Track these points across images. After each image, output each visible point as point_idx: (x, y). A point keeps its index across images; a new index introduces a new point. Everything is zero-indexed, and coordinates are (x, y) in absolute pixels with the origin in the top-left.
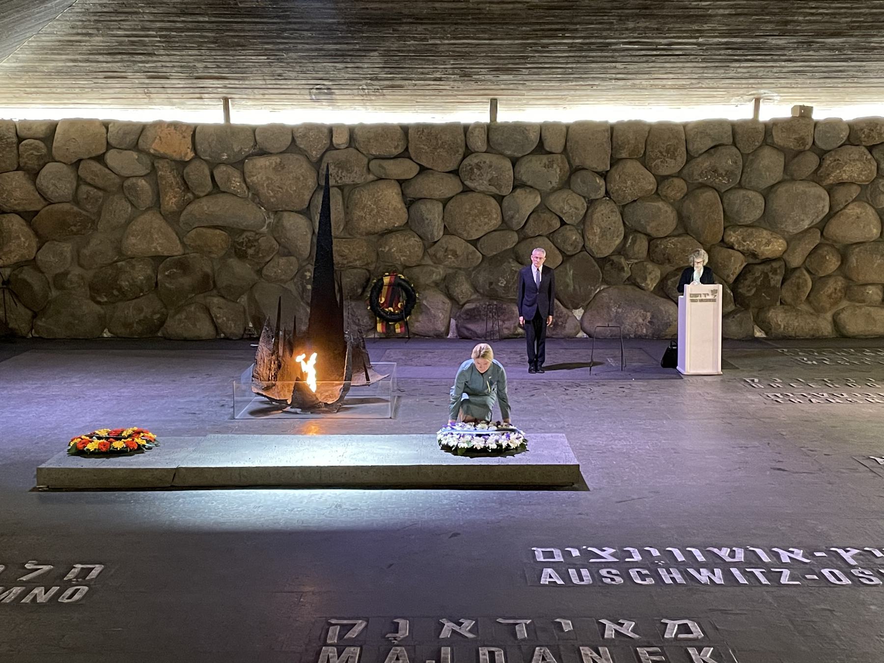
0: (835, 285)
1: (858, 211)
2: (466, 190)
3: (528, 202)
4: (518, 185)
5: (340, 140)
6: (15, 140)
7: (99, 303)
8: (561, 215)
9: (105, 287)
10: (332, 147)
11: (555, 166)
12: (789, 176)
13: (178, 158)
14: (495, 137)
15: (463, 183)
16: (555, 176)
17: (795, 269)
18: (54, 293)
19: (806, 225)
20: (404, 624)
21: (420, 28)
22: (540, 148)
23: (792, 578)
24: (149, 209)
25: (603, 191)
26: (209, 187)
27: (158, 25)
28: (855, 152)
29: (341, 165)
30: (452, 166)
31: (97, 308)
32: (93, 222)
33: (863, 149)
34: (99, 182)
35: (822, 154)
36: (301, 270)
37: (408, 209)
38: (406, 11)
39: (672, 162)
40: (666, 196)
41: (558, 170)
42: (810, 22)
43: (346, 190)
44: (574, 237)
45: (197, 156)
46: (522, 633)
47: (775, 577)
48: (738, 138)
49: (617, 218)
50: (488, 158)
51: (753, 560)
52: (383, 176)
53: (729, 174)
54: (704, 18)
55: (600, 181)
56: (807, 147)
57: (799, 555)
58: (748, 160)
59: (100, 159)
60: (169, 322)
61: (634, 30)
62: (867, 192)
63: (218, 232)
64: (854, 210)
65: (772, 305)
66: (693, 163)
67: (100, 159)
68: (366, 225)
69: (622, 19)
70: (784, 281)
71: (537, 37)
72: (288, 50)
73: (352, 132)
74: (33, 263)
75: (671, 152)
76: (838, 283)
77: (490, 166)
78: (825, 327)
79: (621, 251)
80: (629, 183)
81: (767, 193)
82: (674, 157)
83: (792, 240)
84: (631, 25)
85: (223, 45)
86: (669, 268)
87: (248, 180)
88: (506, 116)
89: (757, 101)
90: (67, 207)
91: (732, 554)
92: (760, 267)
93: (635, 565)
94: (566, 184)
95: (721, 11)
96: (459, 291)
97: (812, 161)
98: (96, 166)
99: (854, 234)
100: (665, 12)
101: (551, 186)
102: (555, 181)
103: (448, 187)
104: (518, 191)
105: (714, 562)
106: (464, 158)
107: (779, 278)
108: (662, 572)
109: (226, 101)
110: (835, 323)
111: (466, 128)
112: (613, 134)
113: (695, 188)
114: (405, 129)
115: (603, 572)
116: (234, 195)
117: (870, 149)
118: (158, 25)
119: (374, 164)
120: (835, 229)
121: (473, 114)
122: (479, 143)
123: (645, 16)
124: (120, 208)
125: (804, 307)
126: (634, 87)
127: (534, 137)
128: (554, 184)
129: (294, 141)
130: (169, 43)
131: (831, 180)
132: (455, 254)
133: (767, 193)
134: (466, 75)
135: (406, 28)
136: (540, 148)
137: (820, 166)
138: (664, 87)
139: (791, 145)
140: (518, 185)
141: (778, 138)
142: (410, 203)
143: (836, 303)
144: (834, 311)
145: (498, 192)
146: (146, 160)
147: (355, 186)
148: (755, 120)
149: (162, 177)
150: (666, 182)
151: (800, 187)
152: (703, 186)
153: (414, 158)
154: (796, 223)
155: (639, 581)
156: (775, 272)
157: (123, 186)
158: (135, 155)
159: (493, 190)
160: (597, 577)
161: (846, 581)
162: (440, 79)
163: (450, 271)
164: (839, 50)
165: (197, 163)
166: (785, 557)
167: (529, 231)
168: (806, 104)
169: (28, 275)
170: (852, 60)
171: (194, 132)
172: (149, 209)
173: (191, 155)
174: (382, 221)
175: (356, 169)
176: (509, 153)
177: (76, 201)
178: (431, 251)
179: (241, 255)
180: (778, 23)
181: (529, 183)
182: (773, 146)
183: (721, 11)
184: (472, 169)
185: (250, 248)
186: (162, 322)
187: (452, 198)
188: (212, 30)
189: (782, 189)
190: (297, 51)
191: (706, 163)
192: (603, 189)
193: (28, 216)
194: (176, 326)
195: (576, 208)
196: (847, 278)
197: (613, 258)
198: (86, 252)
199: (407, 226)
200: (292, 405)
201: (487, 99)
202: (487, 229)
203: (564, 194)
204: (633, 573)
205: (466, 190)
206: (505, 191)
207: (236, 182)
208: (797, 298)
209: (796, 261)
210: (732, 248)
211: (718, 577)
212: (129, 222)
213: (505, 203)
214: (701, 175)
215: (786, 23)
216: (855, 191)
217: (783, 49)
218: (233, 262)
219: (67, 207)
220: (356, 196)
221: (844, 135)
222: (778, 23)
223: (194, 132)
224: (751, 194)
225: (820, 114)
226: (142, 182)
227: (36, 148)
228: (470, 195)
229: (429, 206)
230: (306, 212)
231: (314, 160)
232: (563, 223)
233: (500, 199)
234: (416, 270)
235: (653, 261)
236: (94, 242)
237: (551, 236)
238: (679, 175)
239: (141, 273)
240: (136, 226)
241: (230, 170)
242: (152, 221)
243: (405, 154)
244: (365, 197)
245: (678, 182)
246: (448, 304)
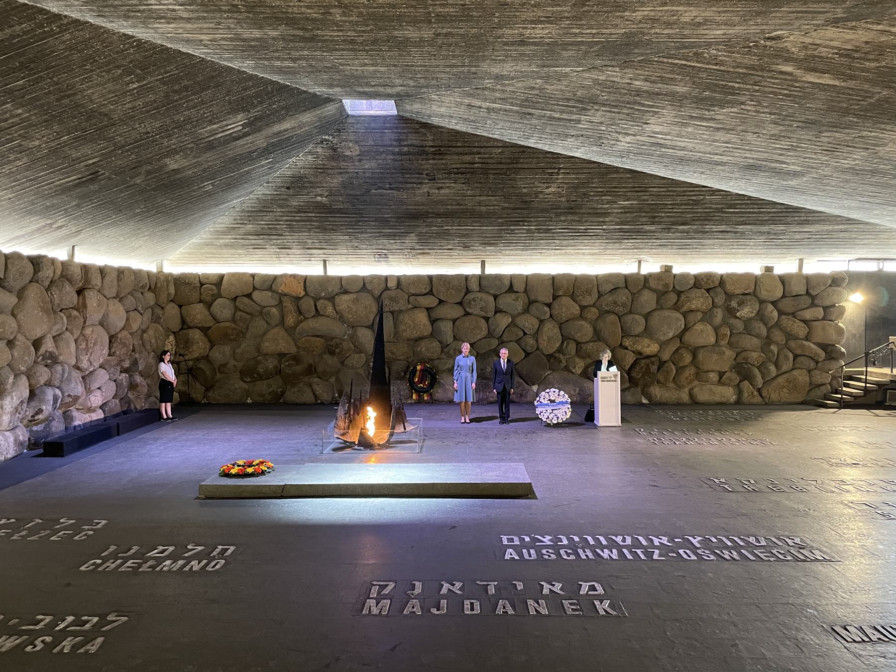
0: (690, 372)
1: (702, 327)
2: (467, 314)
3: (503, 321)
4: (498, 311)
5: (392, 284)
6: (199, 285)
7: (245, 382)
9: (249, 373)
10: (387, 288)
12: (660, 307)
13: (294, 294)
14: (483, 283)
17: (665, 362)
18: (218, 376)
19: (671, 335)
20: (418, 585)
21: (439, 220)
22: (511, 289)
23: (660, 555)
24: (276, 326)
26: (313, 313)
27: (285, 218)
28: (699, 292)
29: (392, 299)
31: (245, 385)
32: (243, 333)
33: (703, 291)
34: (248, 310)
35: (679, 293)
36: (367, 361)
38: (431, 211)
39: (589, 298)
42: (668, 217)
44: (532, 342)
45: (307, 294)
46: (492, 590)
47: (649, 555)
48: (629, 284)
49: (557, 330)
50: (479, 295)
51: (637, 544)
53: (624, 305)
54: (606, 214)
55: (547, 309)
56: (671, 289)
57: (665, 540)
58: (634, 296)
59: (249, 296)
60: (287, 394)
61: (565, 221)
62: (707, 316)
64: (699, 327)
65: (652, 383)
66: (602, 298)
67: (249, 296)
68: (406, 335)
69: (557, 215)
70: (658, 370)
71: (508, 225)
72: (362, 233)
73: (399, 279)
74: (206, 358)
75: (589, 292)
76: (692, 370)
78: (685, 397)
79: (560, 350)
81: (647, 316)
82: (590, 295)
83: (663, 344)
84: (563, 218)
85: (323, 229)
86: (589, 361)
88: (490, 270)
89: (640, 262)
90: (228, 324)
91: (624, 540)
92: (644, 361)
93: (564, 547)
95: (616, 211)
97: (673, 297)
98: (246, 300)
99: (701, 342)
100: (582, 211)
102: (520, 309)
103: (457, 312)
104: (498, 314)
105: (612, 545)
106: (466, 295)
107: (656, 367)
108: (580, 551)
109: (325, 261)
110: (691, 395)
111: (467, 278)
112: (554, 281)
113: (604, 313)
114: (430, 278)
115: (544, 551)
117: (708, 290)
118: (285, 218)
119: (412, 299)
120: (688, 337)
121: (471, 269)
122: (474, 286)
123: (571, 213)
124: (259, 325)
125: (672, 385)
126: (565, 254)
127: (507, 283)
129: (364, 285)
130: (291, 229)
131: (685, 309)
133: (647, 316)
134: (466, 247)
135: (430, 220)
136: (511, 289)
137: (678, 300)
138: (584, 254)
139: (660, 288)
140: (498, 311)
141: (652, 284)
142: (433, 322)
143: (691, 382)
144: (690, 387)
146: (276, 296)
147: (400, 311)
148: (638, 274)
149: (286, 307)
150: (586, 310)
151: (666, 313)
152: (608, 312)
154: (664, 334)
155: (566, 557)
156: (653, 363)
157: (262, 312)
158: (270, 294)
159: (483, 313)
160: (539, 554)
161: (694, 557)
162: (451, 249)
164: (687, 233)
165: (306, 298)
166: (656, 542)
167: (505, 338)
168: (669, 264)
169: (202, 365)
170: (694, 238)
171: (305, 281)
172: (276, 326)
173: (303, 293)
177: (234, 321)
178: (446, 350)
179: (332, 353)
180: (649, 217)
182: (649, 288)
183: (616, 211)
186: (283, 393)
188: (317, 221)
189: (656, 314)
190: (367, 233)
191: (610, 298)
193: (205, 330)
194: (291, 395)
196: (697, 368)
197: (557, 355)
198: (238, 351)
200: (359, 445)
201: (479, 261)
202: (479, 337)
203: (526, 316)
204: (562, 552)
205: (467, 314)
206: (490, 314)
207: (330, 310)
208: (666, 379)
209: (666, 356)
210: (627, 349)
211: (615, 555)
212: (265, 333)
213: (490, 322)
214: (607, 305)
215: (654, 217)
216: (699, 316)
217: (654, 232)
218: (327, 357)
219: (228, 324)
220: (401, 317)
221: (692, 282)
222: (649, 217)
223: (305, 282)
224: (637, 317)
225: (676, 271)
226: (274, 310)
227: (212, 290)
228: (469, 317)
229: (445, 323)
230: (370, 327)
232: (525, 334)
233: (487, 319)
234: (437, 361)
235: (579, 356)
236: (243, 345)
237: (518, 341)
238: (594, 305)
239: (271, 364)
240: (269, 336)
241: (326, 302)
242: (278, 333)
243: (430, 293)
244: (406, 318)
245: (593, 309)
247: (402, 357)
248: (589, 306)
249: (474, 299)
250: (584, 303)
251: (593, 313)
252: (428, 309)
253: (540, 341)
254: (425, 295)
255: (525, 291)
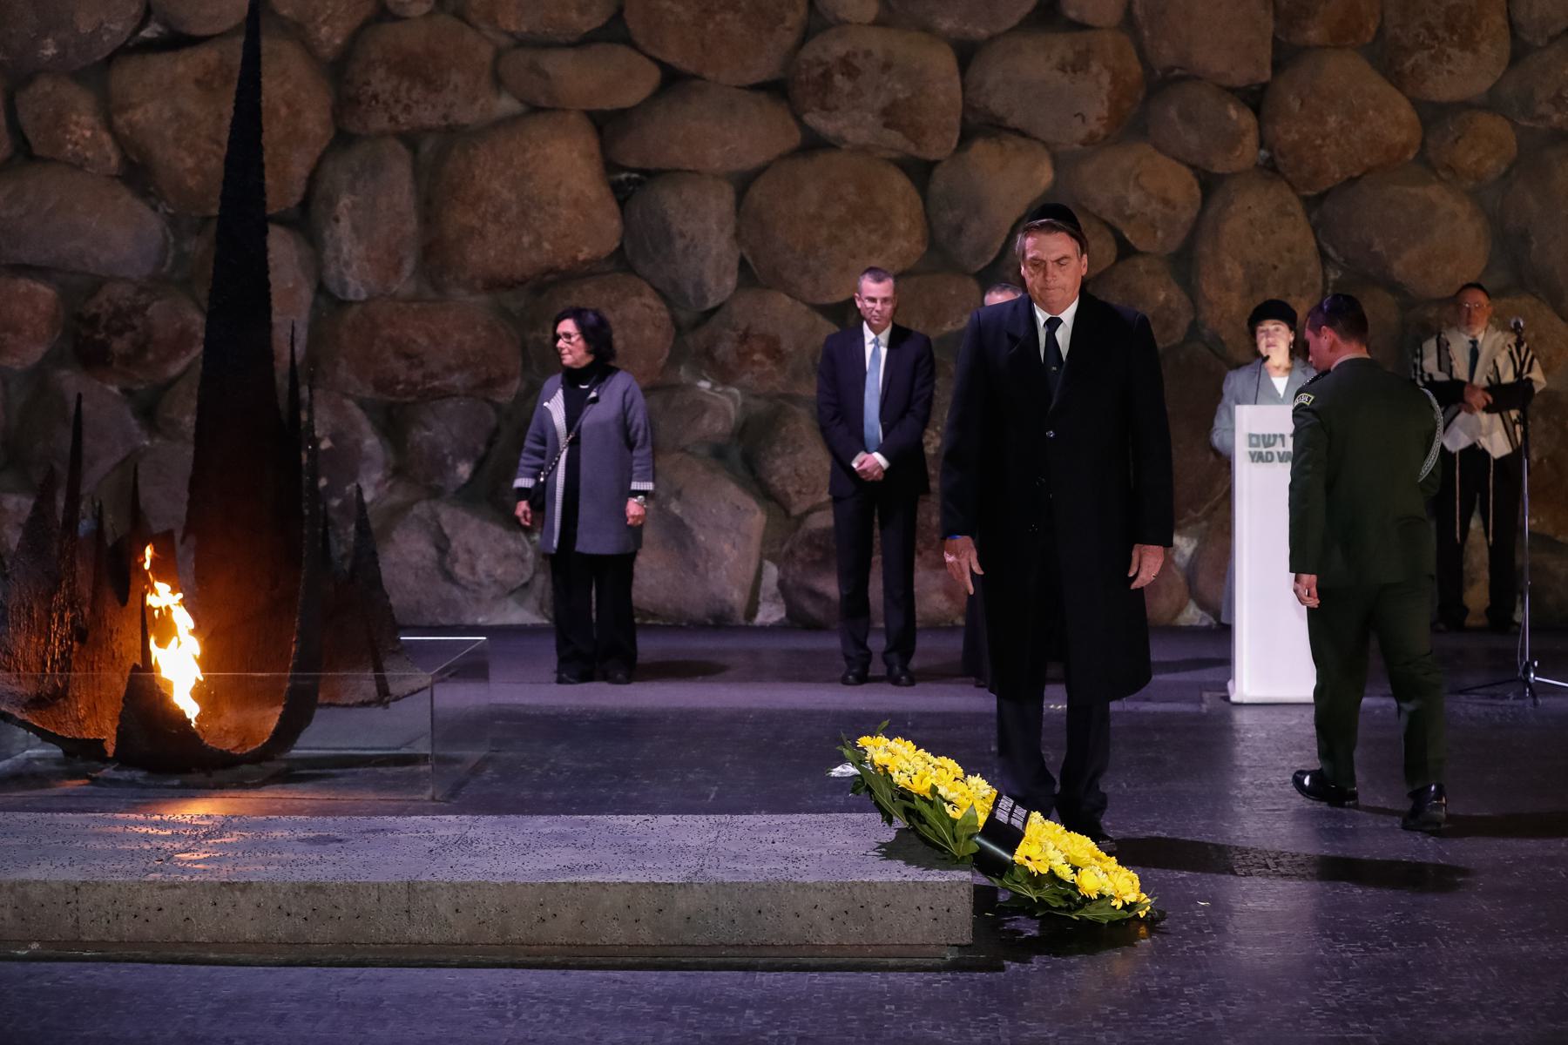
2: (813, 144)
4: (979, 125)
8: (1119, 224)
11: (1095, 67)
15: (798, 119)
16: (1093, 101)
25: (1249, 152)
30: (764, 67)
37: (622, 204)
40: (1450, 168)
41: (1105, 79)
43: (427, 147)
50: (876, 42)
52: (543, 101)
63: (23, 285)
68: (489, 252)
77: (887, 67)
80: (1332, 121)
82: (1468, 43)
87: (120, 121)
94: (1132, 123)
96: (785, 471)
101: (1081, 133)
102: (1097, 111)
104: (979, 147)
116: (78, 165)
128: (1095, 126)
132: (774, 351)
142: (629, 186)
145: (912, 149)
147: (452, 133)
153: (641, 41)
159: (896, 140)
163: (760, 406)
174: (537, 244)
175: (456, 78)
176: (946, 24)
181: (1014, 121)
184: (827, 76)
185: (119, 333)
187: (759, 172)
192: (1251, 140)
195: (1166, 202)
199: (622, 261)
200: (124, 758)
205: (813, 144)
206: (938, 146)
213: (939, 183)
231: (327, 51)
232: (1126, 250)
233: (920, 171)
238: (1492, 103)
243: (614, 32)
246: (756, 518)
247: (457, 380)
248: (1466, 105)
249: (848, 67)
250: (1444, 86)
251: (1486, 147)
252: (607, 126)
253: (1209, 289)
254: (585, 41)
255: (1129, 23)
